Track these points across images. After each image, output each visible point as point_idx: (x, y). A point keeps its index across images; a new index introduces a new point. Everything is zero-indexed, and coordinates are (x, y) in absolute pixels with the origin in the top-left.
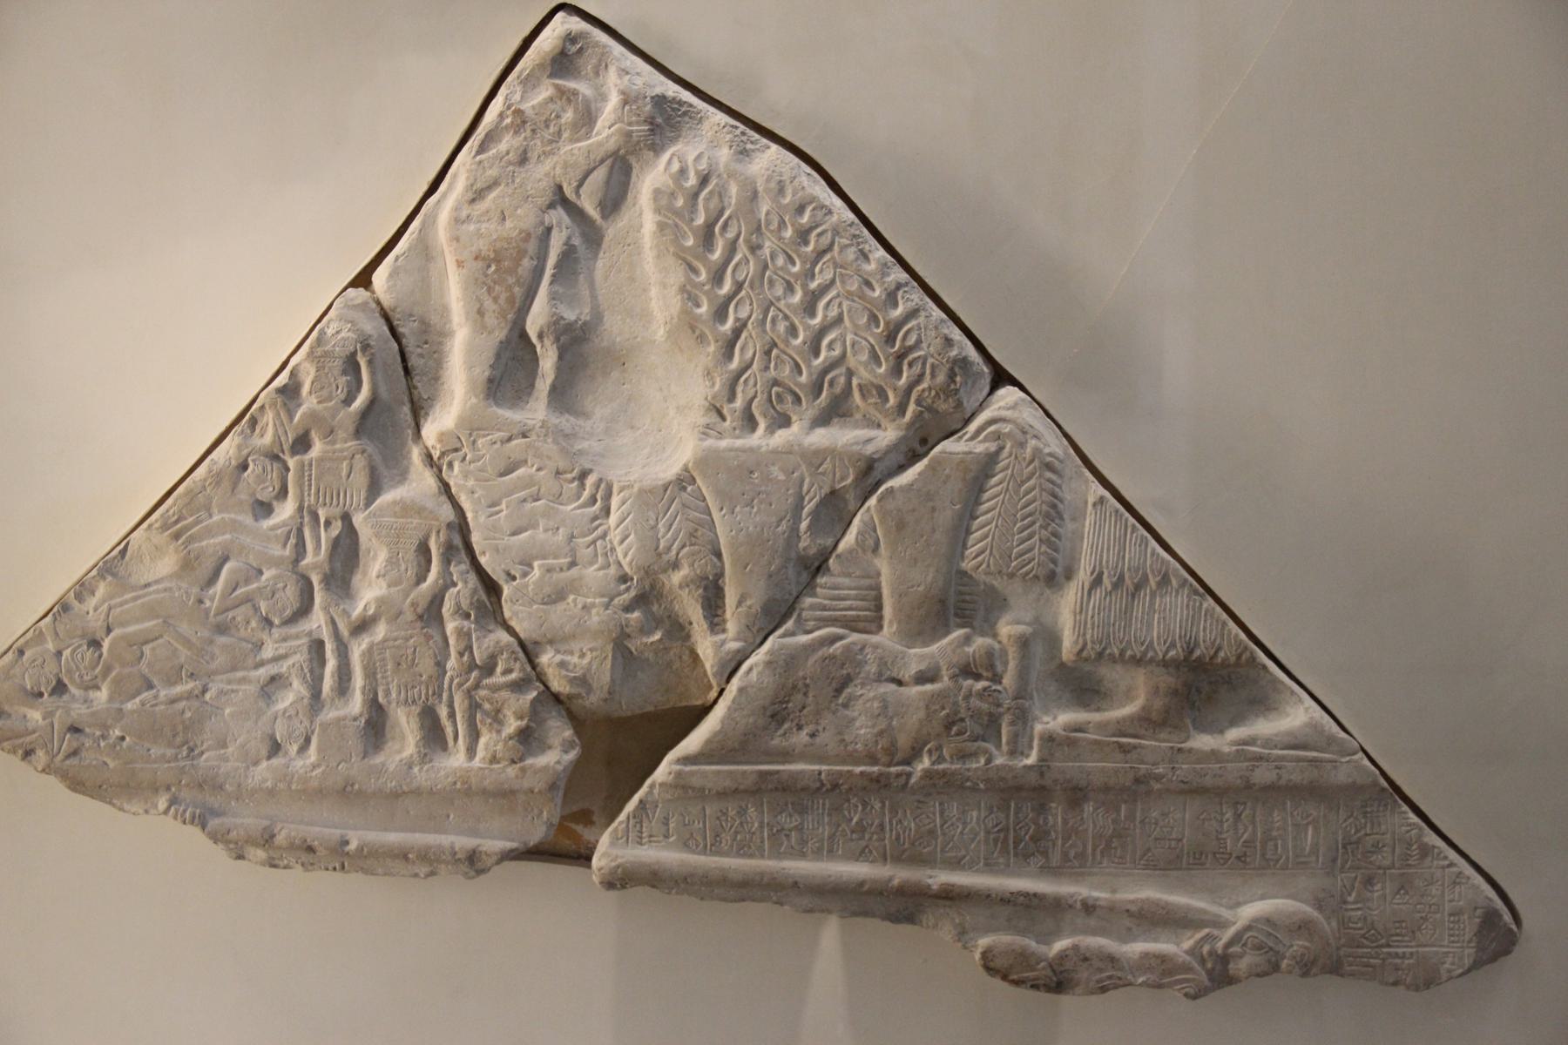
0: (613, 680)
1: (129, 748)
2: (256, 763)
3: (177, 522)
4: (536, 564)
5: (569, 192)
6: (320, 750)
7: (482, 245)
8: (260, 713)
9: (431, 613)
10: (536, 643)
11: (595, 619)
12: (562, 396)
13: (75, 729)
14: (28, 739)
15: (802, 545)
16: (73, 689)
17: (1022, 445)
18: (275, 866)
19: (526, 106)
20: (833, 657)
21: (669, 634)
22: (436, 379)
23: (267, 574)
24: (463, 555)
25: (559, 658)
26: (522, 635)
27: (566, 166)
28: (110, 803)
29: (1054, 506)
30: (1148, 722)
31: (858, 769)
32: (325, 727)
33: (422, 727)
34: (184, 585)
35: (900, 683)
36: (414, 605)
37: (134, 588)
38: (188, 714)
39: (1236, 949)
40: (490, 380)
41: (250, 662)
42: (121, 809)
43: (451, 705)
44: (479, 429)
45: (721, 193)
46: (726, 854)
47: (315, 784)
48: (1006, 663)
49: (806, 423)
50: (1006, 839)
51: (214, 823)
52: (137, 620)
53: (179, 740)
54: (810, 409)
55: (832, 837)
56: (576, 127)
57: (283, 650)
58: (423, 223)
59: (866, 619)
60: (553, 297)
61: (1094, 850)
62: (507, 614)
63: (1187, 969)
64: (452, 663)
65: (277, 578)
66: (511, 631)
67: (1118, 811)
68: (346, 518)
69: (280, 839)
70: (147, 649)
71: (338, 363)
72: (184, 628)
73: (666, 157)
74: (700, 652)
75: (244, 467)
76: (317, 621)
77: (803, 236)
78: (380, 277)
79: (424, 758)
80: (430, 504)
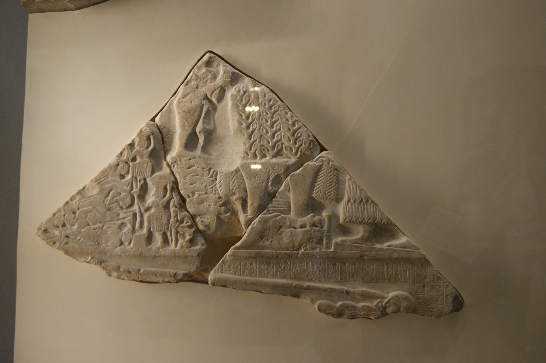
0: (216, 226)
1: (82, 242)
2: (116, 247)
4: (196, 193)
5: (209, 96)
6: (134, 244)
7: (185, 109)
8: (118, 233)
9: (167, 206)
10: (195, 215)
11: (212, 209)
12: (204, 149)
13: (67, 237)
15: (269, 189)
16: (68, 226)
17: (329, 163)
18: (119, 278)
19: (199, 74)
20: (277, 220)
21: (232, 214)
22: (171, 143)
23: (122, 194)
24: (176, 190)
25: (201, 220)
26: (191, 213)
27: (208, 89)
28: (75, 258)
29: (337, 180)
30: (363, 240)
31: (284, 252)
32: (136, 237)
33: (163, 238)
34: (100, 197)
35: (295, 228)
36: (162, 203)
38: (98, 233)
39: (388, 305)
40: (186, 144)
41: (116, 219)
42: (78, 260)
43: (171, 232)
45: (249, 96)
46: (247, 276)
47: (132, 253)
48: (324, 223)
49: (271, 157)
50: (325, 273)
51: (103, 264)
52: (86, 206)
54: (272, 153)
55: (276, 272)
56: (211, 79)
57: (125, 215)
58: (170, 104)
59: (286, 211)
60: (204, 122)
61: (349, 276)
62: (188, 207)
63: (375, 310)
64: (172, 220)
66: (188, 212)
67: (355, 265)
68: (145, 179)
69: (122, 269)
70: (88, 214)
71: (145, 138)
72: (99, 208)
73: (235, 87)
74: (240, 219)
75: (118, 165)
76: (135, 207)
77: (271, 108)
78: (157, 119)
79: (163, 247)
80: (168, 176)
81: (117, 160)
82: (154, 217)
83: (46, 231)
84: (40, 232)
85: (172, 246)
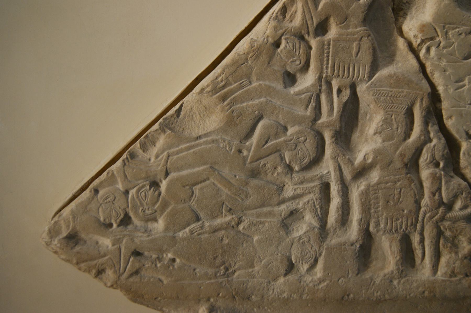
1: (180, 268)
2: (275, 279)
3: (224, 87)
6: (325, 269)
13: (137, 254)
14: (101, 261)
16: (136, 221)
23: (291, 131)
32: (330, 250)
33: (401, 250)
34: (227, 138)
36: (402, 155)
37: (188, 140)
38: (226, 241)
41: (275, 200)
43: (422, 234)
44: (450, 24)
53: (218, 261)
62: (463, 162)
64: (426, 201)
65: (299, 133)
66: (464, 178)
68: (353, 87)
70: (196, 189)
72: (226, 172)
75: (277, 44)
76: (327, 167)
79: (401, 274)
80: (414, 79)
81: (275, 28)
82: (380, 194)
83: (73, 238)
84: (56, 242)
85: (424, 272)
